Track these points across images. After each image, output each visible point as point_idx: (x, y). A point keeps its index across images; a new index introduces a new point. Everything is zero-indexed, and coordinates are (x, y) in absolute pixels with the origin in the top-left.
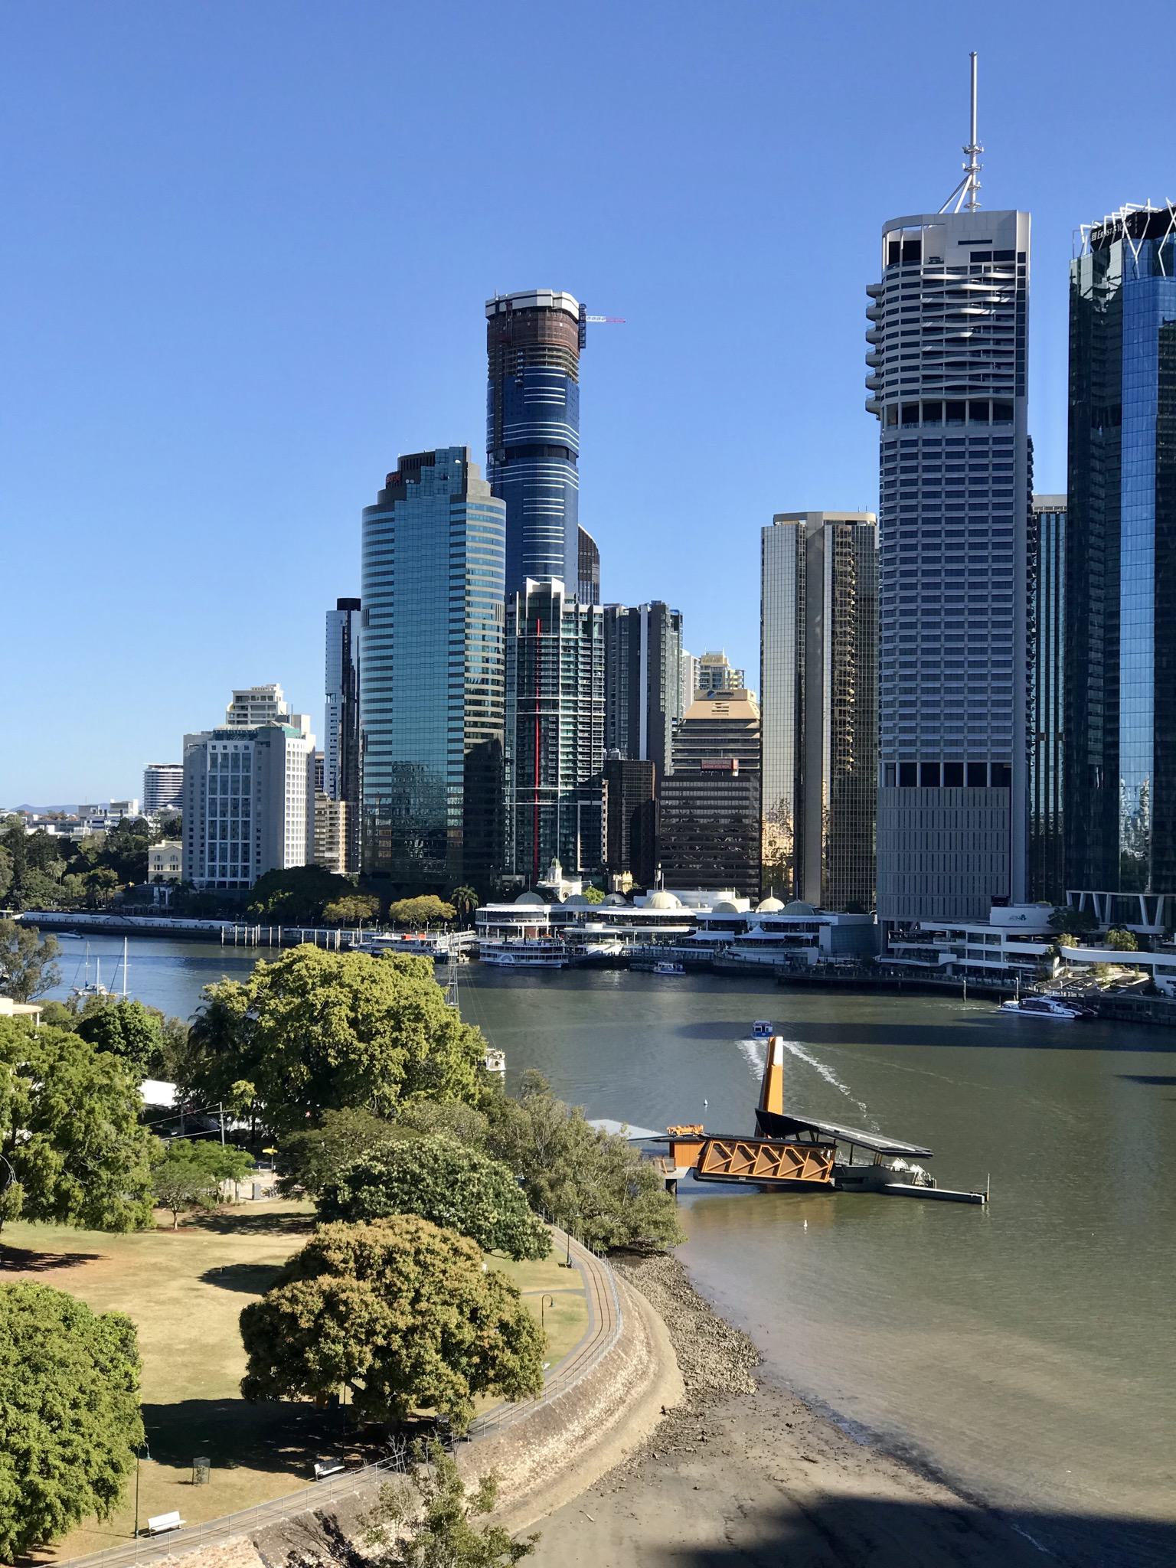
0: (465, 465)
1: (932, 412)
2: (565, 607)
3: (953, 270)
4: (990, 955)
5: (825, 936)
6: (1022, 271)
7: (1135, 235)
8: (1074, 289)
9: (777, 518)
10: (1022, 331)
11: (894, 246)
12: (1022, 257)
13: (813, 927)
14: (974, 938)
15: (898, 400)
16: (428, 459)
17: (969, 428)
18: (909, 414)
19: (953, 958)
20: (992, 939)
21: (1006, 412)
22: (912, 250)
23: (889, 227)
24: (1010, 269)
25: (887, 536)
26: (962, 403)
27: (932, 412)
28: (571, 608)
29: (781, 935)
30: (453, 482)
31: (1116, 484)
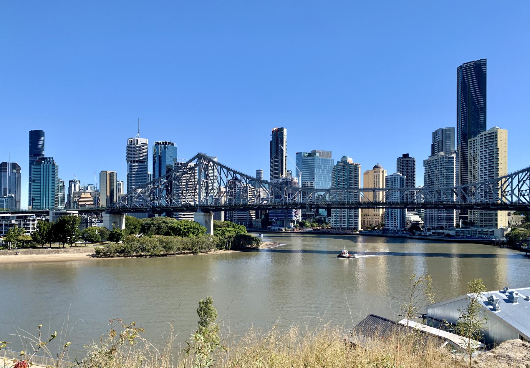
7: (163, 144)
15: (132, 160)
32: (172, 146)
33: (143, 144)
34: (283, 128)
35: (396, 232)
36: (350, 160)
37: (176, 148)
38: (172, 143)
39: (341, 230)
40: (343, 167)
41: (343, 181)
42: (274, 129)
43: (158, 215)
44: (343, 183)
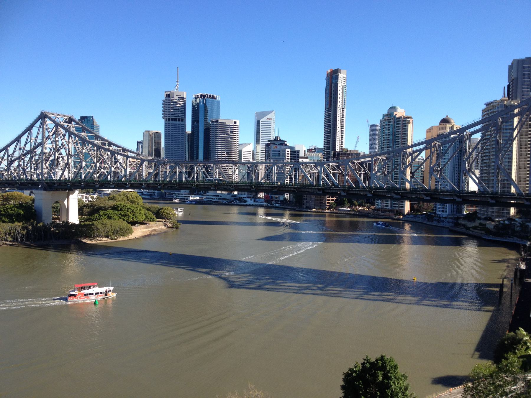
0: (93, 119)
3: (175, 99)
4: (181, 196)
5: (156, 194)
7: (201, 98)
9: (145, 131)
10: (185, 109)
11: (167, 94)
12: (185, 98)
13: (154, 193)
14: (179, 194)
15: (167, 117)
16: (86, 117)
17: (177, 122)
18: (169, 119)
19: (176, 197)
20: (182, 194)
21: (182, 120)
22: (169, 95)
23: (166, 92)
27: (172, 119)
29: (149, 194)
30: (91, 121)
32: (212, 99)
33: (180, 98)
34: (338, 69)
35: (442, 219)
36: (400, 113)
37: (219, 102)
38: (213, 96)
39: (380, 212)
40: (389, 122)
41: (388, 142)
42: (329, 71)
43: (92, 190)
44: (388, 145)
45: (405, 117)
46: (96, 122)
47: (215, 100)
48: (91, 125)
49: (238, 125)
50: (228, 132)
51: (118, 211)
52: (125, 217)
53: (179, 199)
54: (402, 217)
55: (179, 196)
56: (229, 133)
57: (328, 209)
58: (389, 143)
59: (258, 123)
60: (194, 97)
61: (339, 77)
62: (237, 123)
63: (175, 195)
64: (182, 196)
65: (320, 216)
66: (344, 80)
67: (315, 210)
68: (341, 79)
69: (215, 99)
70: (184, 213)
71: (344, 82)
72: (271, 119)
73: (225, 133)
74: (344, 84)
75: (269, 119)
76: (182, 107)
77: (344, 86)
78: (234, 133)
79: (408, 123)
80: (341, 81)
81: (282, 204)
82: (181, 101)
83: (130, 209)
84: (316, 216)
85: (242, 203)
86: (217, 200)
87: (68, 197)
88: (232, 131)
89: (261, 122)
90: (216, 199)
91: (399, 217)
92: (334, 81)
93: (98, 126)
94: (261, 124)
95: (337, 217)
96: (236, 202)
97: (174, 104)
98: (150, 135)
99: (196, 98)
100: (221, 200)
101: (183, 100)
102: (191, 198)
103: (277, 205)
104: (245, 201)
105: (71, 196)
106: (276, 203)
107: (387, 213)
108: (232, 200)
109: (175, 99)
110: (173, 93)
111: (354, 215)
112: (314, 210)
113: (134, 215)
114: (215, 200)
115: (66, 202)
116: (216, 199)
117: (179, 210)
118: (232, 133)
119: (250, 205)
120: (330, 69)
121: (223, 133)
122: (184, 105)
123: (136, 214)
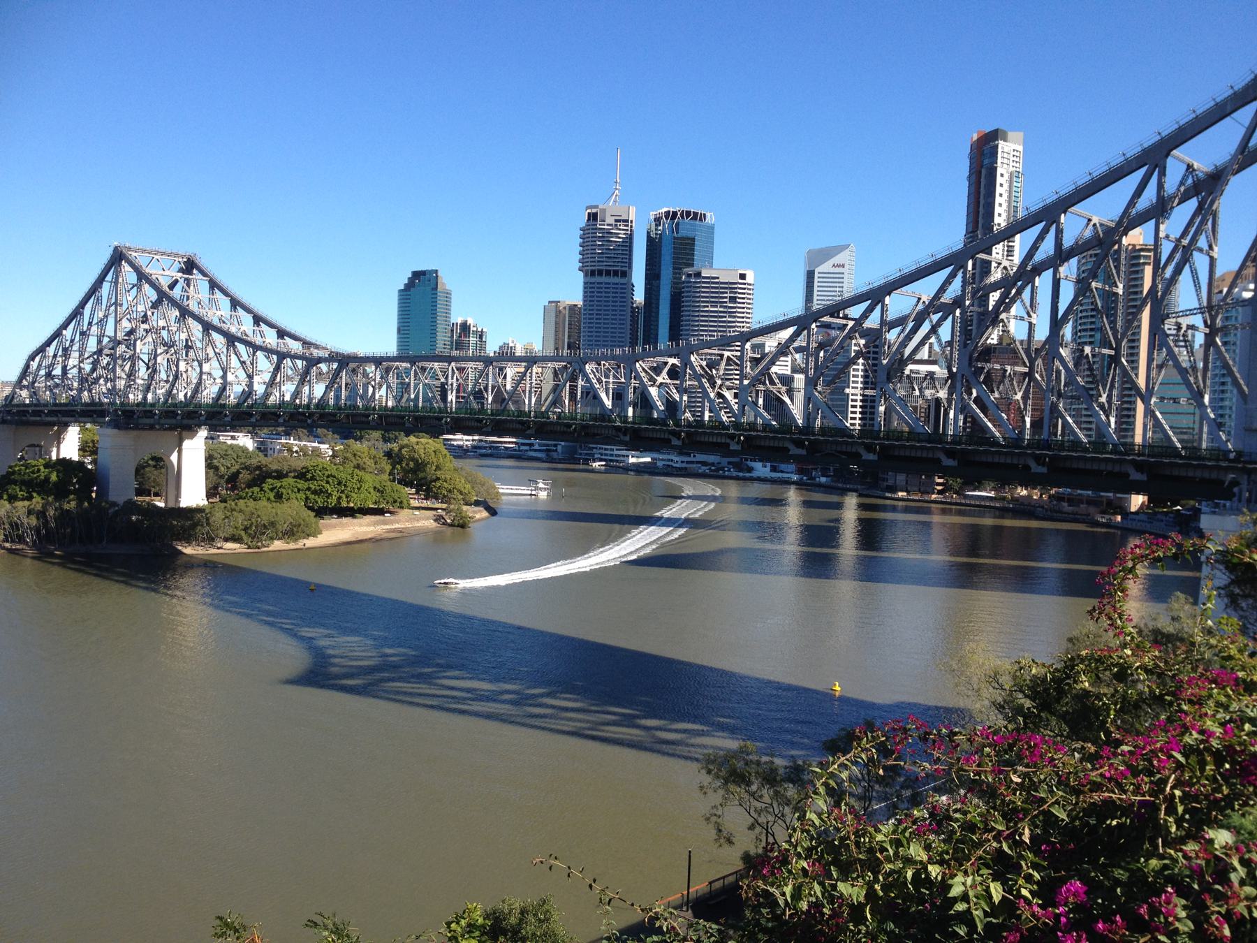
0: (437, 276)
1: (600, 273)
2: (472, 329)
3: (608, 225)
6: (631, 227)
7: (667, 219)
8: (648, 233)
9: (550, 302)
11: (589, 214)
13: (556, 446)
14: (606, 449)
15: (589, 268)
16: (423, 273)
18: (593, 273)
19: (599, 456)
23: (588, 208)
24: (627, 226)
25: (585, 310)
26: (610, 271)
27: (600, 273)
28: (475, 329)
31: (658, 300)
32: (692, 222)
33: (619, 221)
37: (712, 228)
38: (696, 214)
39: (1065, 504)
42: (975, 137)
44: (1092, 323)
45: (1138, 247)
46: (443, 284)
47: (700, 223)
48: (433, 289)
49: (752, 282)
50: (725, 300)
51: (307, 480)
52: (319, 495)
53: (605, 460)
54: (1119, 518)
55: (606, 455)
56: (726, 302)
57: (940, 492)
58: (1093, 320)
59: (810, 276)
60: (652, 218)
61: (1000, 150)
62: (747, 277)
63: (598, 452)
64: (612, 455)
65: (918, 511)
66: (1015, 159)
67: (905, 494)
68: (1006, 155)
69: (701, 220)
70: (553, 496)
71: (1014, 164)
72: (843, 266)
73: (716, 302)
74: (1014, 169)
75: (839, 266)
76: (623, 242)
77: (1016, 174)
78: (739, 303)
79: (1144, 264)
80: (1005, 161)
81: (835, 479)
82: (621, 227)
83: (334, 477)
84: (907, 510)
85: (741, 474)
86: (684, 465)
87: (180, 446)
88: (735, 298)
89: (816, 275)
90: (682, 462)
91: (1112, 517)
92: (986, 162)
93: (448, 294)
94: (816, 280)
95: (960, 513)
96: (729, 471)
97: (606, 235)
98: (560, 312)
99: (658, 220)
100: (695, 465)
101: (625, 226)
102: (632, 460)
103: (823, 480)
104: (750, 470)
105: (187, 444)
106: (823, 476)
107: (1082, 506)
108: (720, 466)
109: (608, 225)
110: (604, 211)
111: (1003, 512)
112: (901, 494)
113: (342, 492)
114: (678, 465)
115: (174, 458)
116: (682, 462)
117: (541, 485)
118: (735, 302)
119: (759, 479)
120: (978, 132)
121: (713, 302)
122: (630, 238)
123: (349, 489)
